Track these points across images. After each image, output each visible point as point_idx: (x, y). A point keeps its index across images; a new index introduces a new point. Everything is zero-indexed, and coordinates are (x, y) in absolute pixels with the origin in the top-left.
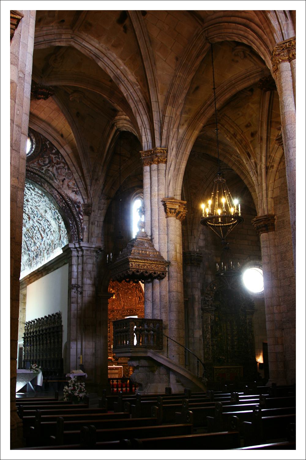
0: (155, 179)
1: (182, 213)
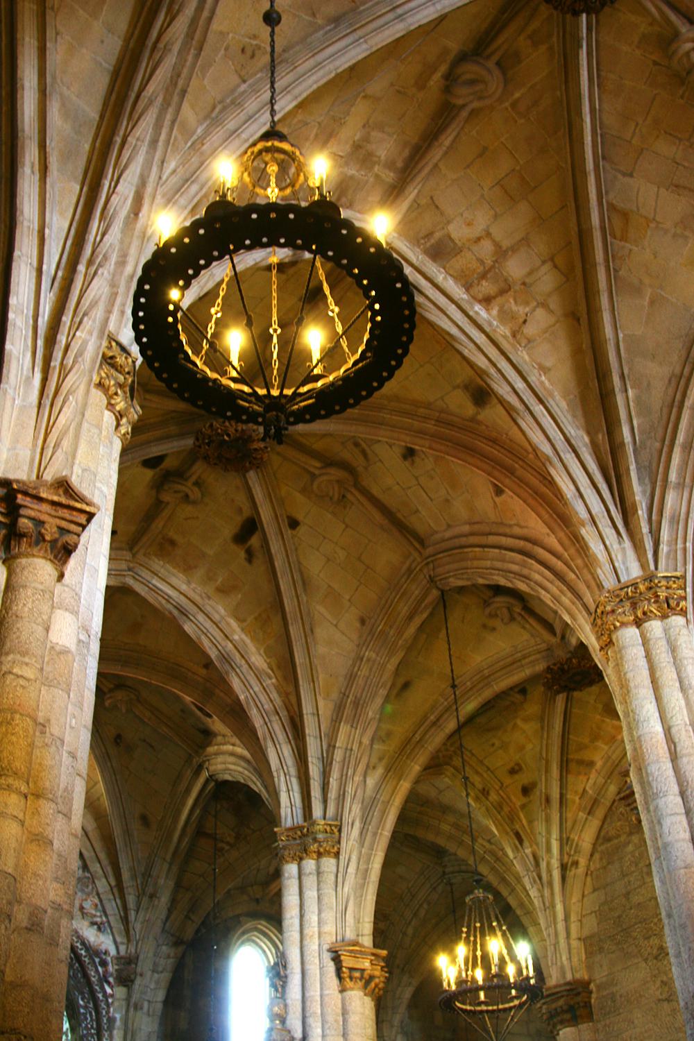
0: (311, 894)
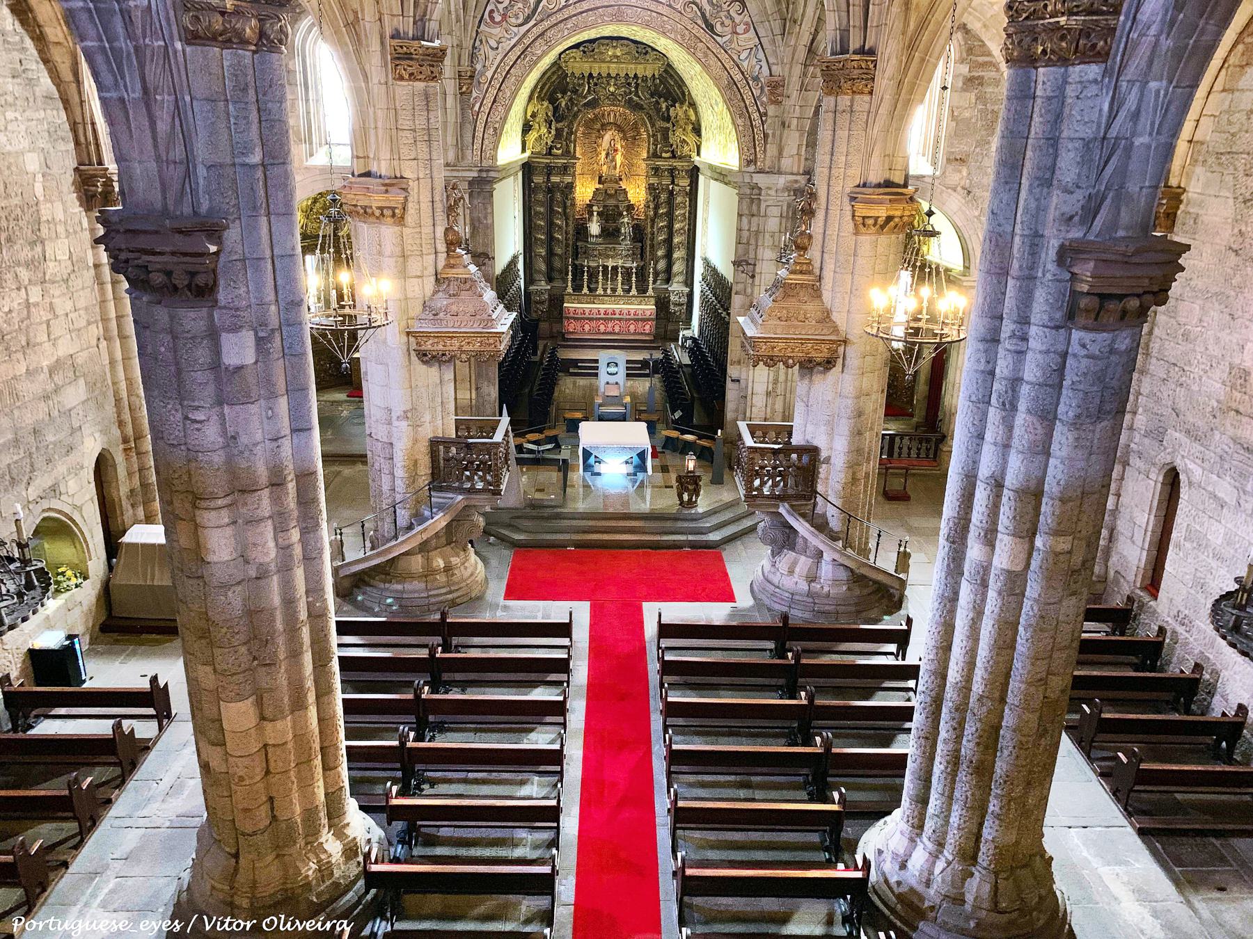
0: (842, 134)
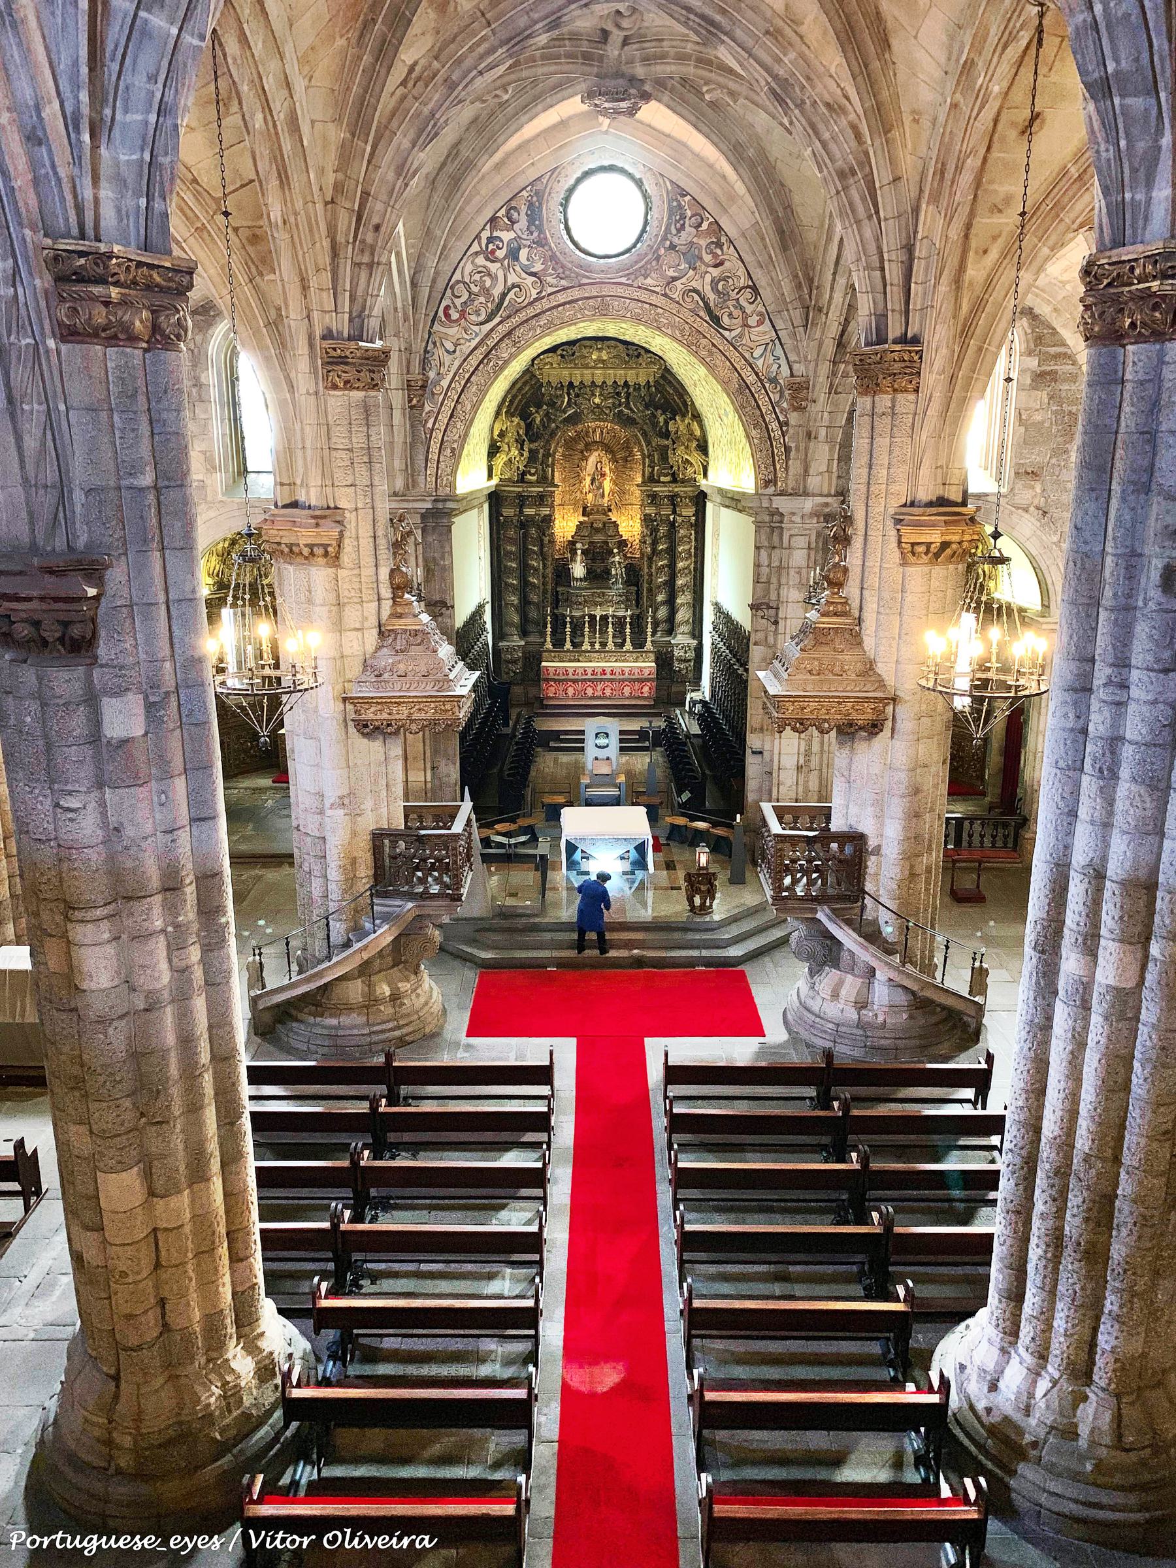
0: (882, 442)
1: (954, 546)
